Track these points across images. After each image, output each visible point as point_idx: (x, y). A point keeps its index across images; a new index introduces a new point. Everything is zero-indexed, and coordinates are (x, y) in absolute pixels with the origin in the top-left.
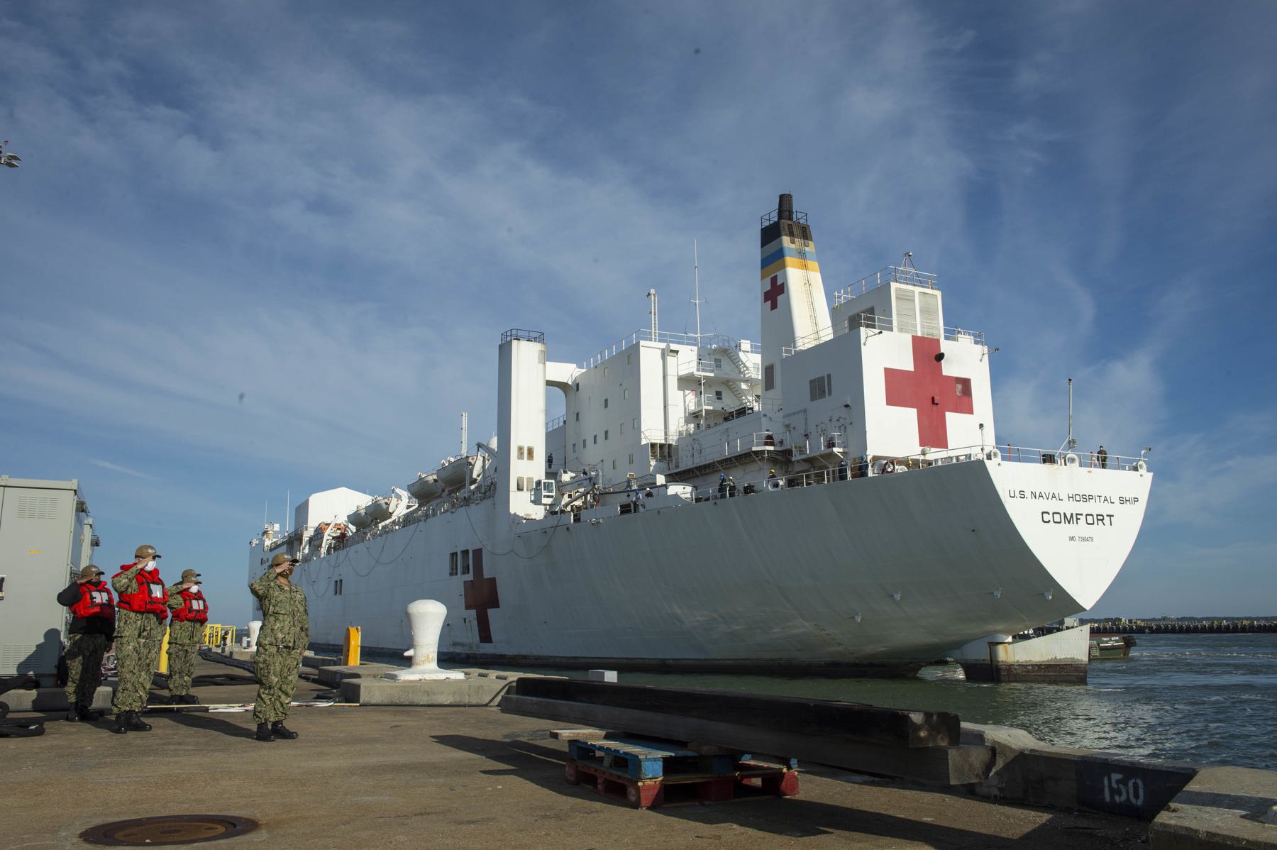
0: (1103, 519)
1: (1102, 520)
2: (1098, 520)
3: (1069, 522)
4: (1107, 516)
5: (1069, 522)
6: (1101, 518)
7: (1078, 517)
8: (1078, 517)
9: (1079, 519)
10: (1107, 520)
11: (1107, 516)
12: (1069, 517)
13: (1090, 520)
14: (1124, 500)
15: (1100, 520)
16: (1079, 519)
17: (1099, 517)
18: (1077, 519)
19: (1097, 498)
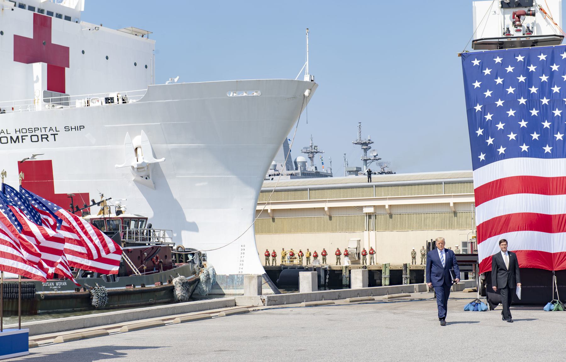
0: (48, 137)
1: (46, 138)
2: (42, 138)
3: (15, 142)
4: (51, 135)
5: (15, 142)
6: (46, 136)
7: (23, 138)
8: (23, 138)
9: (25, 139)
10: (51, 138)
11: (51, 135)
12: (15, 140)
13: (35, 139)
14: (70, 128)
15: (44, 138)
16: (25, 139)
17: (43, 137)
18: (22, 139)
19: (43, 130)
